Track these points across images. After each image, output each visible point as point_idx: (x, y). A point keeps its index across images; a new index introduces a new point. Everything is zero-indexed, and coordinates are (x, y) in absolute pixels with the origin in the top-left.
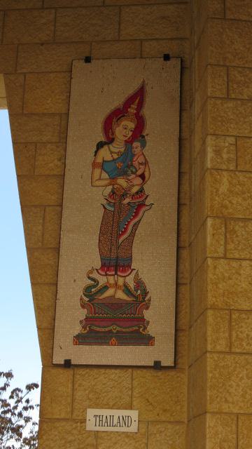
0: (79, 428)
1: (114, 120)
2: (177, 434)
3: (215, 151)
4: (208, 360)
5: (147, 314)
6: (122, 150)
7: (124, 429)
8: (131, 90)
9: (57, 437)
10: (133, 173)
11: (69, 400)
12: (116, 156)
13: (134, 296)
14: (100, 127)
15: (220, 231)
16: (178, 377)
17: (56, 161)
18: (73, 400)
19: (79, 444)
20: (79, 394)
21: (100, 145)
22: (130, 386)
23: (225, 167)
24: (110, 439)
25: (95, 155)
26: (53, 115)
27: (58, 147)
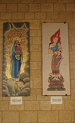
8: (57, 31)
12: (54, 47)
14: (50, 39)
21: (50, 44)
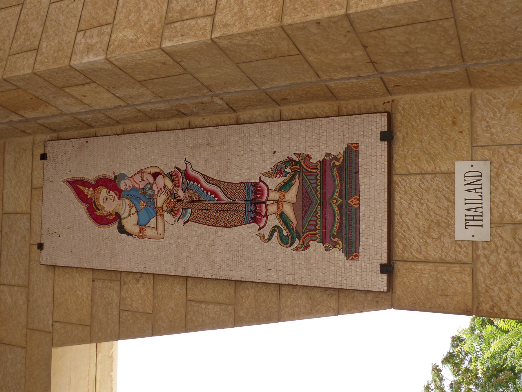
0: (486, 252)
1: (98, 214)
2: (489, 101)
3: (88, 52)
4: (359, 9)
5: (317, 157)
6: (127, 202)
7: (485, 181)
9: (503, 287)
10: (151, 188)
11: (442, 268)
12: (134, 210)
13: (293, 176)
15: (178, 28)
16: (404, 109)
17: (138, 285)
18: (442, 262)
19: (513, 253)
20: (433, 254)
21: (122, 230)
22: (418, 177)
23: (107, 38)
24: (504, 203)
25: (131, 235)
26: (93, 288)
27: (125, 283)
